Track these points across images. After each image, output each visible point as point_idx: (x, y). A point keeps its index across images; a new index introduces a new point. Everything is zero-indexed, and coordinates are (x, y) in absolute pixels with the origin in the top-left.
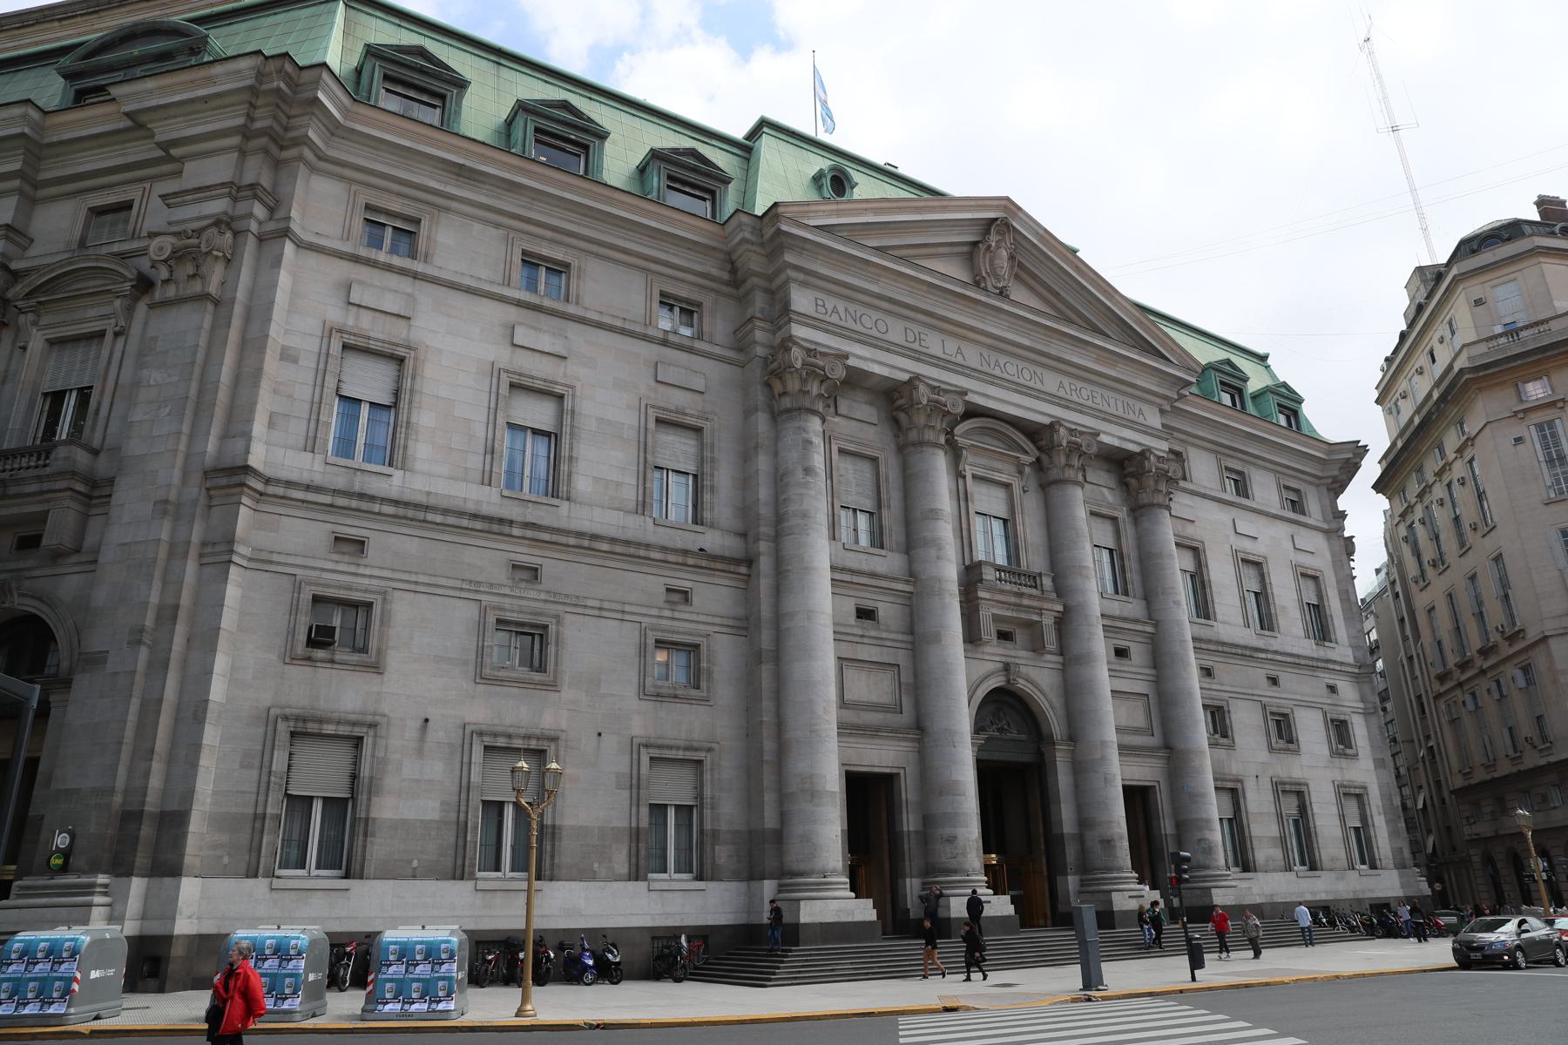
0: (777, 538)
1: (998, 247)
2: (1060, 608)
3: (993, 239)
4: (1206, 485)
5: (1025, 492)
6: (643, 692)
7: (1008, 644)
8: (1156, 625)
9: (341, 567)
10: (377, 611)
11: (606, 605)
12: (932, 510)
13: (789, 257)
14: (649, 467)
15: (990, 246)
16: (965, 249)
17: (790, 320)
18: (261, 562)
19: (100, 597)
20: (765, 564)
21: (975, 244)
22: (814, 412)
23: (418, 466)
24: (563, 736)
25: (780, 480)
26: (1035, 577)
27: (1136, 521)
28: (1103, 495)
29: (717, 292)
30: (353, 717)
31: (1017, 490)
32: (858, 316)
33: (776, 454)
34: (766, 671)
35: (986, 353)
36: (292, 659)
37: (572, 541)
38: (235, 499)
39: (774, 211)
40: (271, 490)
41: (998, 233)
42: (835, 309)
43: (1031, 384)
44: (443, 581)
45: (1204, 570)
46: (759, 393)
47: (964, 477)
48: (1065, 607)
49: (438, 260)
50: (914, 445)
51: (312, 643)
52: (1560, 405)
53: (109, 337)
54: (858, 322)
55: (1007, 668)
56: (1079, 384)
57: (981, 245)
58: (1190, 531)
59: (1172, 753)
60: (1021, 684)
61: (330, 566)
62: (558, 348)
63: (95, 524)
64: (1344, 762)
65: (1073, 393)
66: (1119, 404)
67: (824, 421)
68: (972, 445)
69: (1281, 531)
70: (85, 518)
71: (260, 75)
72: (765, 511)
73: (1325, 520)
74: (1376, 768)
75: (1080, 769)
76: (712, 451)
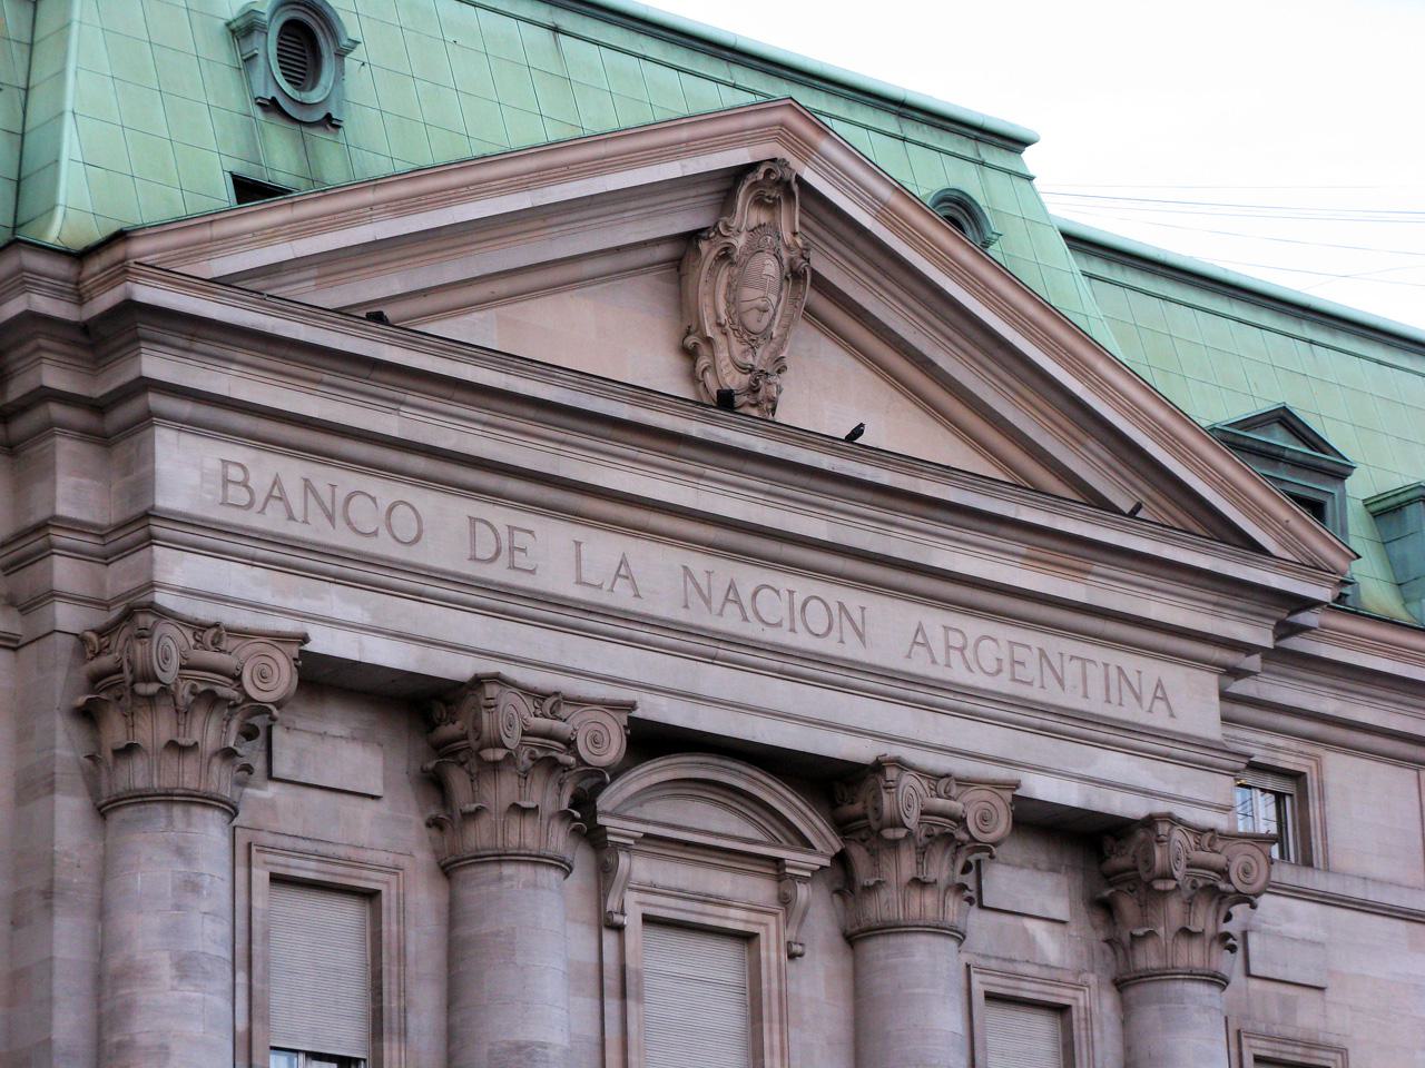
1: (755, 250)
3: (747, 215)
4: (1378, 868)
5: (792, 956)
12: (519, 1048)
13: (155, 364)
15: (726, 256)
16: (662, 253)
17: (150, 540)
21: (691, 238)
27: (1126, 1011)
28: (1030, 941)
31: (770, 952)
32: (341, 495)
33: (102, 912)
35: (699, 562)
39: (118, 252)
41: (759, 202)
42: (277, 493)
43: (829, 647)
46: (61, 738)
47: (619, 929)
50: (480, 859)
54: (339, 521)
56: (973, 627)
57: (704, 246)
65: (956, 656)
66: (1095, 673)
67: (232, 811)
68: (647, 836)
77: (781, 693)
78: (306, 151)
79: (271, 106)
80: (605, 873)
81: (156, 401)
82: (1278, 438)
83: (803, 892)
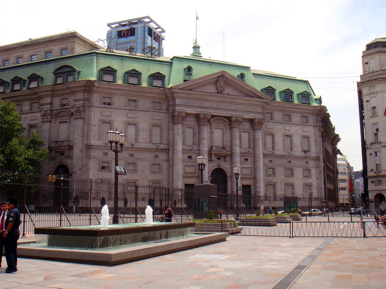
0: (173, 146)
1: (221, 81)
3: (221, 78)
6: (151, 172)
7: (219, 160)
8: (255, 154)
10: (110, 163)
11: (144, 159)
12: (203, 138)
14: (151, 135)
15: (219, 82)
18: (94, 158)
19: (74, 163)
20: (171, 150)
21: (217, 80)
22: (179, 123)
24: (138, 180)
25: (173, 135)
26: (225, 148)
27: (254, 132)
31: (224, 130)
33: (173, 131)
34: (171, 168)
37: (138, 149)
40: (94, 147)
51: (102, 169)
52: (376, 93)
53: (68, 122)
56: (240, 106)
58: (271, 131)
59: (255, 179)
60: (221, 167)
61: (103, 157)
62: (135, 117)
63: (71, 152)
64: (307, 178)
69: (299, 128)
70: (69, 151)
71: (87, 83)
72: (171, 141)
73: (314, 123)
74: (316, 179)
76: (162, 130)
77: (224, 112)
79: (187, 74)
80: (211, 125)
82: (270, 88)
83: (226, 125)
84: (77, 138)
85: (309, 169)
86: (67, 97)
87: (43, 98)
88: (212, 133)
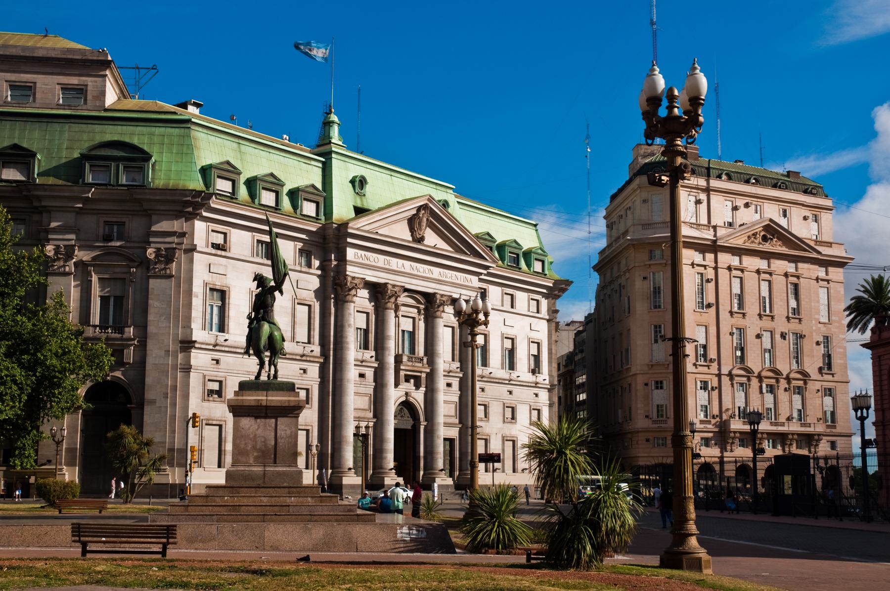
2: (428, 370)
9: (215, 370)
21: (414, 215)
23: (231, 331)
28: (450, 317)
29: (317, 246)
30: (219, 419)
31: (417, 320)
36: (204, 400)
38: (189, 350)
44: (240, 372)
45: (488, 344)
47: (398, 317)
48: (431, 370)
49: (232, 250)
55: (407, 394)
60: (411, 400)
61: (212, 369)
75: (430, 432)
78: (362, 200)
81: (348, 245)
82: (487, 237)
84: (158, 321)
85: (538, 408)
86: (123, 220)
87: (49, 212)
88: (398, 325)
